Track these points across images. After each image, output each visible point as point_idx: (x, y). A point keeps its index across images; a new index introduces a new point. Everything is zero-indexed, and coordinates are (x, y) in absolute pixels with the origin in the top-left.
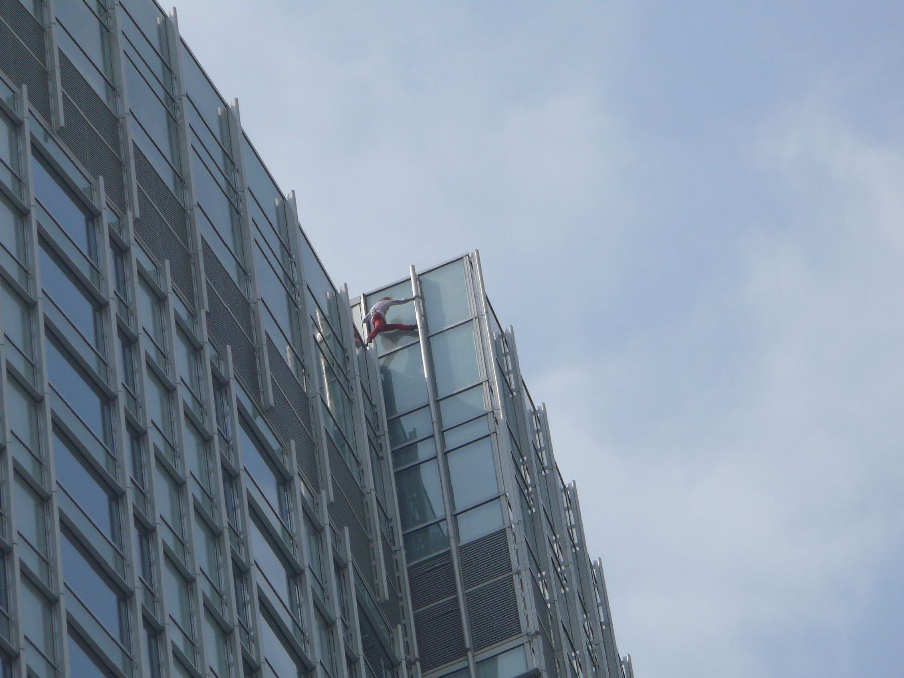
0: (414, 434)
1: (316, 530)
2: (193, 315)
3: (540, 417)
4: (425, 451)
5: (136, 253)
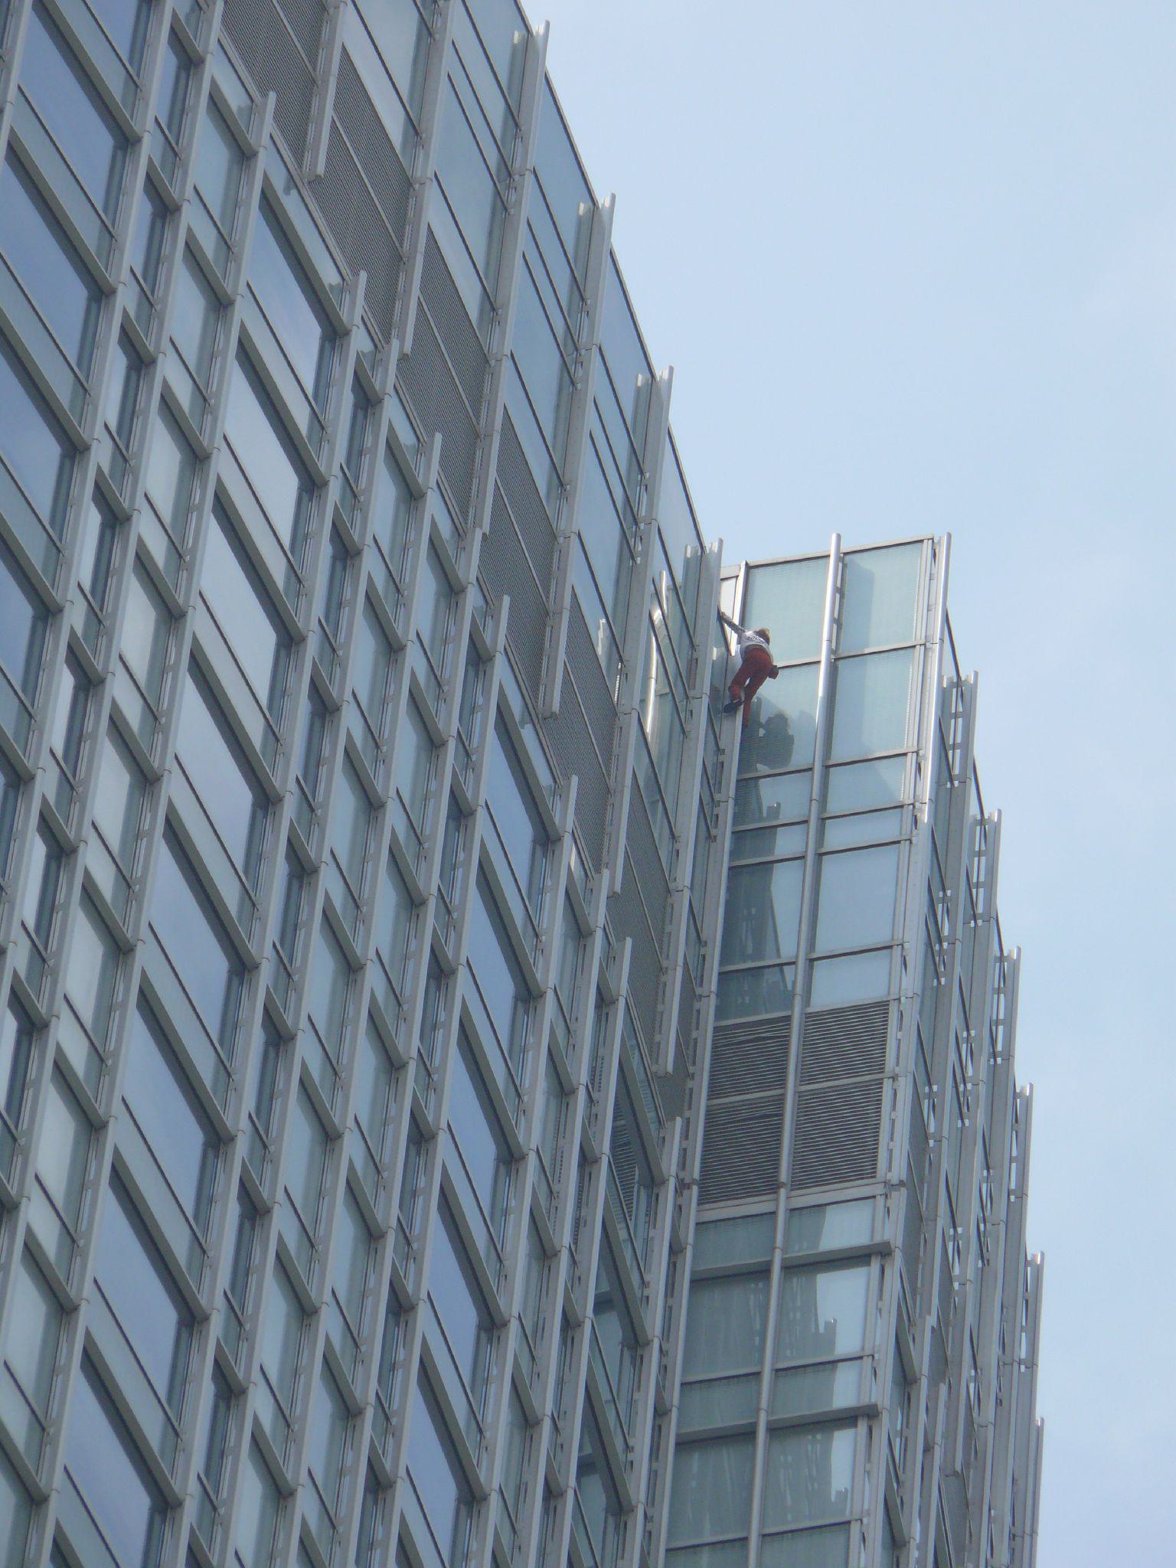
0: (775, 811)
1: (579, 932)
2: (459, 533)
3: (989, 831)
4: (786, 843)
5: (392, 411)
